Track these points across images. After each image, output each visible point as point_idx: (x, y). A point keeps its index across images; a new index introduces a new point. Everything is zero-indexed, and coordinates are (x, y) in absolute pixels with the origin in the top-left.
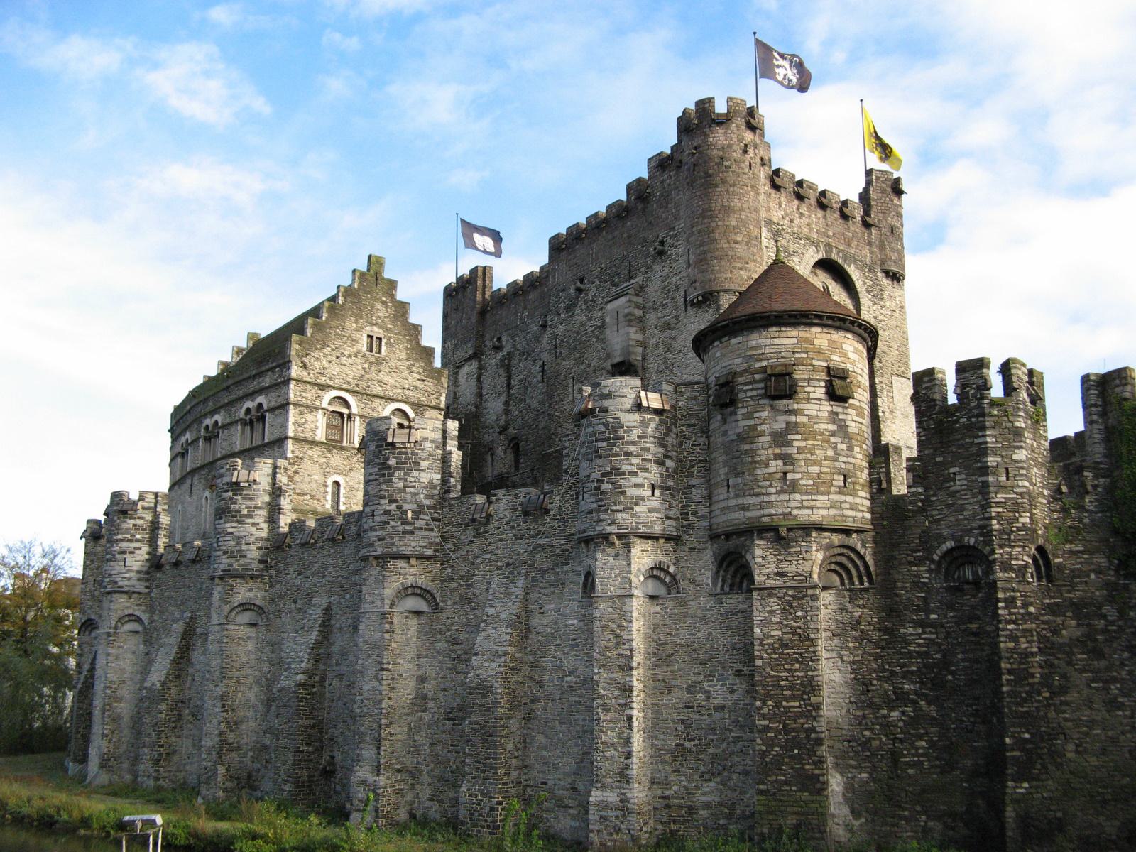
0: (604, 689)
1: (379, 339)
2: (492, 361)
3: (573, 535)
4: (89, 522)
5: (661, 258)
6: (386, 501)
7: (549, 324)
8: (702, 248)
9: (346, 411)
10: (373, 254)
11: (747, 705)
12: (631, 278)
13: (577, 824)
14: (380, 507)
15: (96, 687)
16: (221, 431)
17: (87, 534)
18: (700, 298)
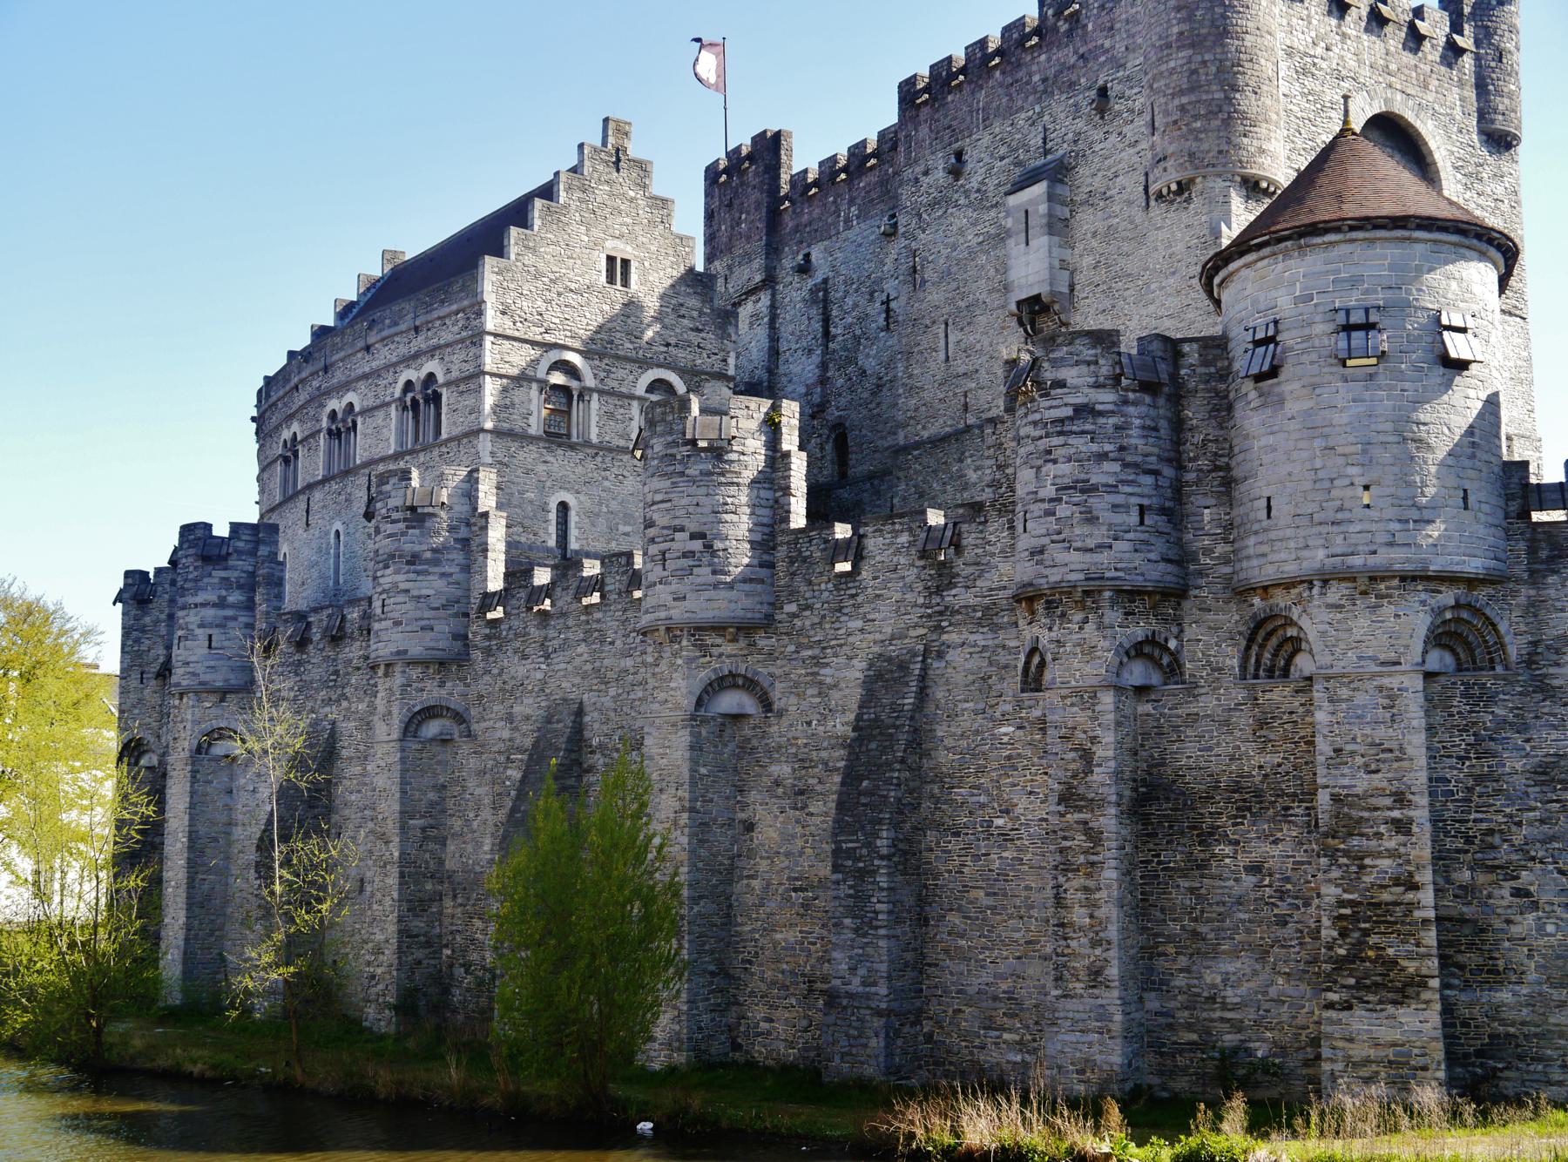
0: (1065, 838)
1: (626, 263)
2: (794, 292)
3: (1005, 588)
4: (128, 574)
5: (1102, 118)
6: (686, 535)
7: (901, 230)
8: (1176, 102)
9: (574, 384)
10: (611, 116)
11: (1302, 863)
12: (1046, 152)
13: (1019, 1058)
14: (674, 545)
15: (167, 849)
16: (359, 420)
17: (125, 596)
18: (1174, 187)
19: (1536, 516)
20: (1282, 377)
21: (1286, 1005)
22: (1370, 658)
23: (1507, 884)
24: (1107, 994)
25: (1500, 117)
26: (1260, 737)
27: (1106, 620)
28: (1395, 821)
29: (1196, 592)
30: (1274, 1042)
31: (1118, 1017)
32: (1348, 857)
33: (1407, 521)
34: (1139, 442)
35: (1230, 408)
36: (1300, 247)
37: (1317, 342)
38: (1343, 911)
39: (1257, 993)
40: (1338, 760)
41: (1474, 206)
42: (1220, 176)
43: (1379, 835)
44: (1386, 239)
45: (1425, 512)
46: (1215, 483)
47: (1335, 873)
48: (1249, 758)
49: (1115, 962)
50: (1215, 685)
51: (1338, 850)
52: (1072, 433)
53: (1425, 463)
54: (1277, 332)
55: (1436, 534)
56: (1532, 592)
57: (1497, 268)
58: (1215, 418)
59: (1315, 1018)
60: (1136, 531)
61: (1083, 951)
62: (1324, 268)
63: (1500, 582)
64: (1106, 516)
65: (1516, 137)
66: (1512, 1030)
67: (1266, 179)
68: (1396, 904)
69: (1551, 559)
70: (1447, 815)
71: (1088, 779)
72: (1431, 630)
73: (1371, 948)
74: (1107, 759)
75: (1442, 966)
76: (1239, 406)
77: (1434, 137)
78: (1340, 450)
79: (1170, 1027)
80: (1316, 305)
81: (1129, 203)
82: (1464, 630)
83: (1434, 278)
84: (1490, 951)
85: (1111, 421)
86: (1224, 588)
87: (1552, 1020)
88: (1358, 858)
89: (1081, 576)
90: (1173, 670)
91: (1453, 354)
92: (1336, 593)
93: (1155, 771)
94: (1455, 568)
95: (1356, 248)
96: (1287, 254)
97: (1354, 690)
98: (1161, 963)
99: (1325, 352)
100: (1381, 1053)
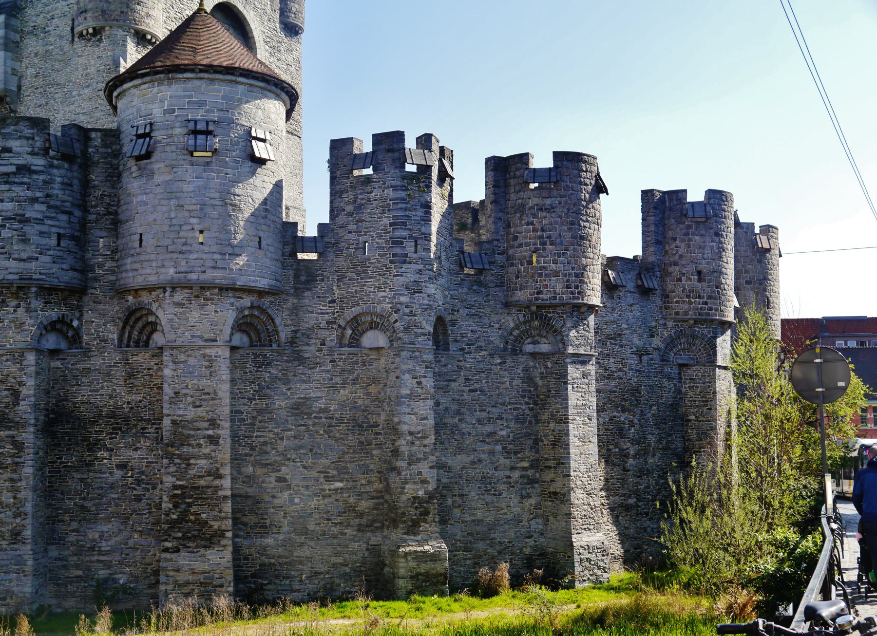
11: (152, 462)
19: (300, 256)
20: (153, 159)
21: (139, 550)
22: (199, 337)
23: (273, 475)
24: (23, 548)
25: (293, 15)
26: (129, 384)
27: (32, 306)
28: (209, 437)
29: (92, 291)
30: (131, 574)
31: (30, 563)
32: (181, 459)
33: (225, 254)
34: (61, 192)
35: (119, 176)
36: (169, 79)
37: (176, 139)
38: (176, 492)
39: (121, 544)
40: (177, 399)
41: (275, 66)
42: (121, 27)
43: (199, 445)
44: (221, 80)
45: (236, 249)
46: (107, 222)
47: (172, 469)
48: (122, 397)
49: (29, 527)
50: (101, 350)
51: (174, 454)
52: (15, 183)
53: (238, 219)
54: (151, 130)
55: (241, 263)
56: (295, 301)
57: (285, 105)
58: (110, 181)
59: (157, 558)
60: (54, 250)
61: (8, 520)
62: (182, 93)
63: (277, 294)
64: (35, 239)
65: (301, 28)
66: (273, 561)
67: (150, 33)
68: (208, 487)
69: (308, 282)
70: (241, 433)
71: (17, 408)
72: (236, 321)
73: (192, 514)
74: (29, 396)
75: (234, 524)
76: (125, 175)
77: (254, 21)
78: (186, 207)
79: (65, 567)
80: (176, 116)
81: (61, 37)
82: (255, 321)
83: (248, 107)
84: (262, 514)
85: (42, 177)
86: (110, 289)
87: (295, 554)
88: (186, 459)
89: (17, 277)
90: (75, 340)
91: (257, 155)
92: (179, 296)
93: (61, 404)
94: (252, 284)
95: (203, 84)
96: (160, 84)
97: (188, 356)
98: (61, 527)
99: (180, 146)
100: (196, 578)
